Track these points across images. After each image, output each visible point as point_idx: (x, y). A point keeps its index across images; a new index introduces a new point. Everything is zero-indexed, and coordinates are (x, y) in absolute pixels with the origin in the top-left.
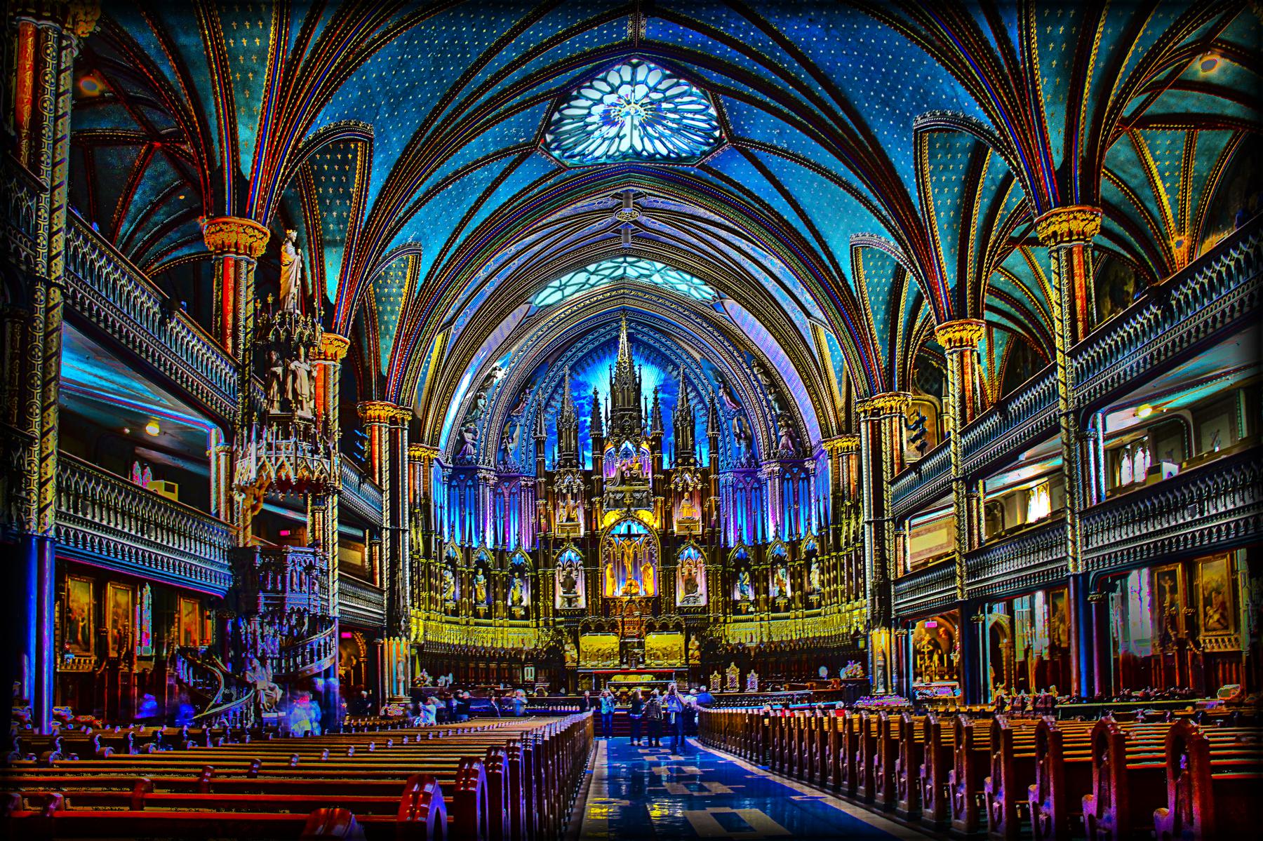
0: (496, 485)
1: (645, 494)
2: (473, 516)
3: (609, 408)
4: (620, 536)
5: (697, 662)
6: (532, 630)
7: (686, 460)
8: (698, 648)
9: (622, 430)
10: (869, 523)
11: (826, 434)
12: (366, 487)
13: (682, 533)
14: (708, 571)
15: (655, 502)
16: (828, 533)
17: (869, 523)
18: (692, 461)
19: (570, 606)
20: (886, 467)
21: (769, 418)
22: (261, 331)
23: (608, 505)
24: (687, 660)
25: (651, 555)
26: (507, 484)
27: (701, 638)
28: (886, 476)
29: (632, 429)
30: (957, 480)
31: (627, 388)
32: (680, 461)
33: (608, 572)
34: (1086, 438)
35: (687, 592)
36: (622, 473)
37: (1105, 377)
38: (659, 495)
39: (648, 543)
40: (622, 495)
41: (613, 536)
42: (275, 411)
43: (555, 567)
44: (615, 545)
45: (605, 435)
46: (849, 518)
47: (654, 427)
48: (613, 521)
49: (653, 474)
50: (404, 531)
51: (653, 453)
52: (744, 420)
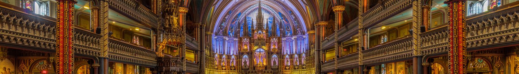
0: (228, 40)
1: (264, 43)
2: (222, 47)
4: (258, 52)
7: (274, 35)
9: (259, 28)
10: (316, 50)
11: (308, 30)
12: (193, 42)
15: (266, 45)
16: (308, 52)
17: (316, 50)
18: (276, 35)
20: (321, 38)
22: (163, 8)
23: (255, 45)
25: (265, 56)
28: (321, 40)
29: (261, 28)
30: (336, 42)
31: (260, 18)
34: (365, 35)
36: (259, 38)
37: (369, 21)
39: (265, 54)
41: (256, 52)
42: (167, 26)
45: (255, 29)
46: (313, 49)
47: (266, 28)
48: (256, 48)
50: (204, 51)
52: (289, 26)
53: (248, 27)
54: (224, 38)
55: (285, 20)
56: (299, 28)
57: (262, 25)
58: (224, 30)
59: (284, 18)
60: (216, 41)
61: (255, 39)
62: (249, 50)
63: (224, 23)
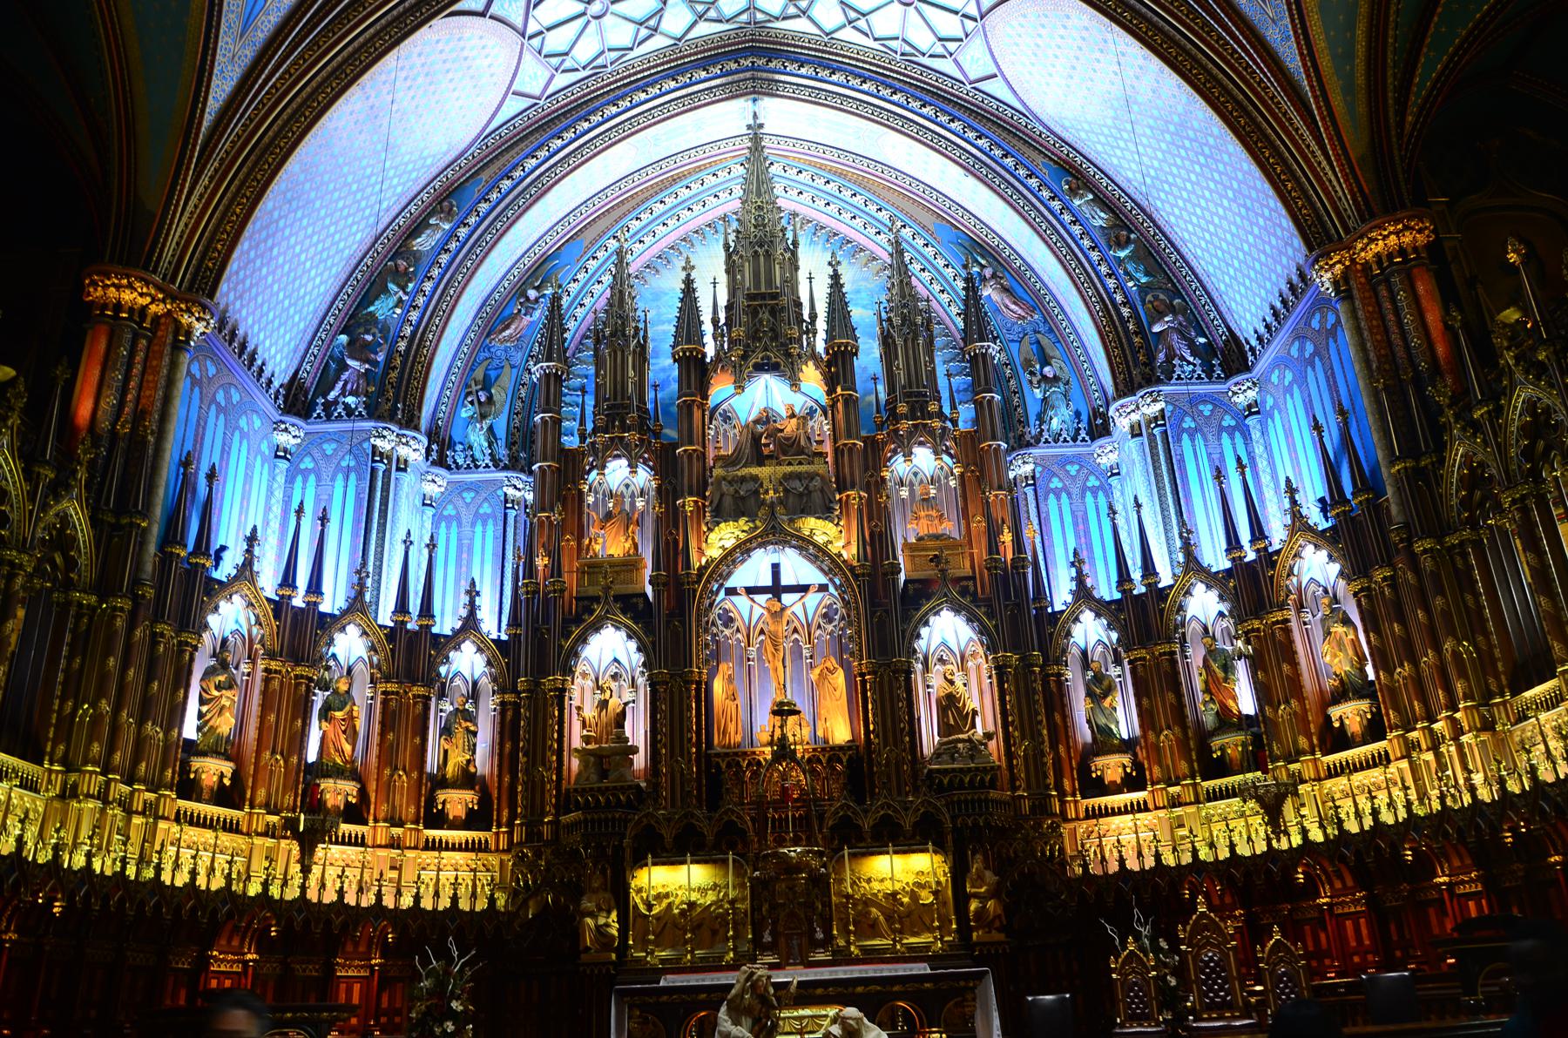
0: (447, 497)
3: (723, 300)
4: (750, 591)
5: (997, 936)
6: (493, 860)
8: (994, 893)
13: (916, 575)
14: (1000, 670)
15: (845, 505)
18: (933, 408)
19: (603, 774)
21: (1119, 298)
24: (964, 930)
26: (468, 496)
27: (1000, 865)
32: (902, 408)
33: (718, 686)
35: (945, 729)
36: (756, 439)
38: (853, 487)
39: (827, 617)
40: (751, 486)
41: (732, 592)
43: (568, 671)
44: (738, 623)
45: (710, 350)
49: (835, 441)
51: (829, 393)
52: (1045, 341)
53: (643, 347)
54: (384, 445)
55: (1005, 290)
56: (1172, 310)
57: (784, 300)
58: (389, 358)
59: (988, 272)
60: (290, 481)
61: (717, 458)
62: (648, 572)
63: (392, 286)
